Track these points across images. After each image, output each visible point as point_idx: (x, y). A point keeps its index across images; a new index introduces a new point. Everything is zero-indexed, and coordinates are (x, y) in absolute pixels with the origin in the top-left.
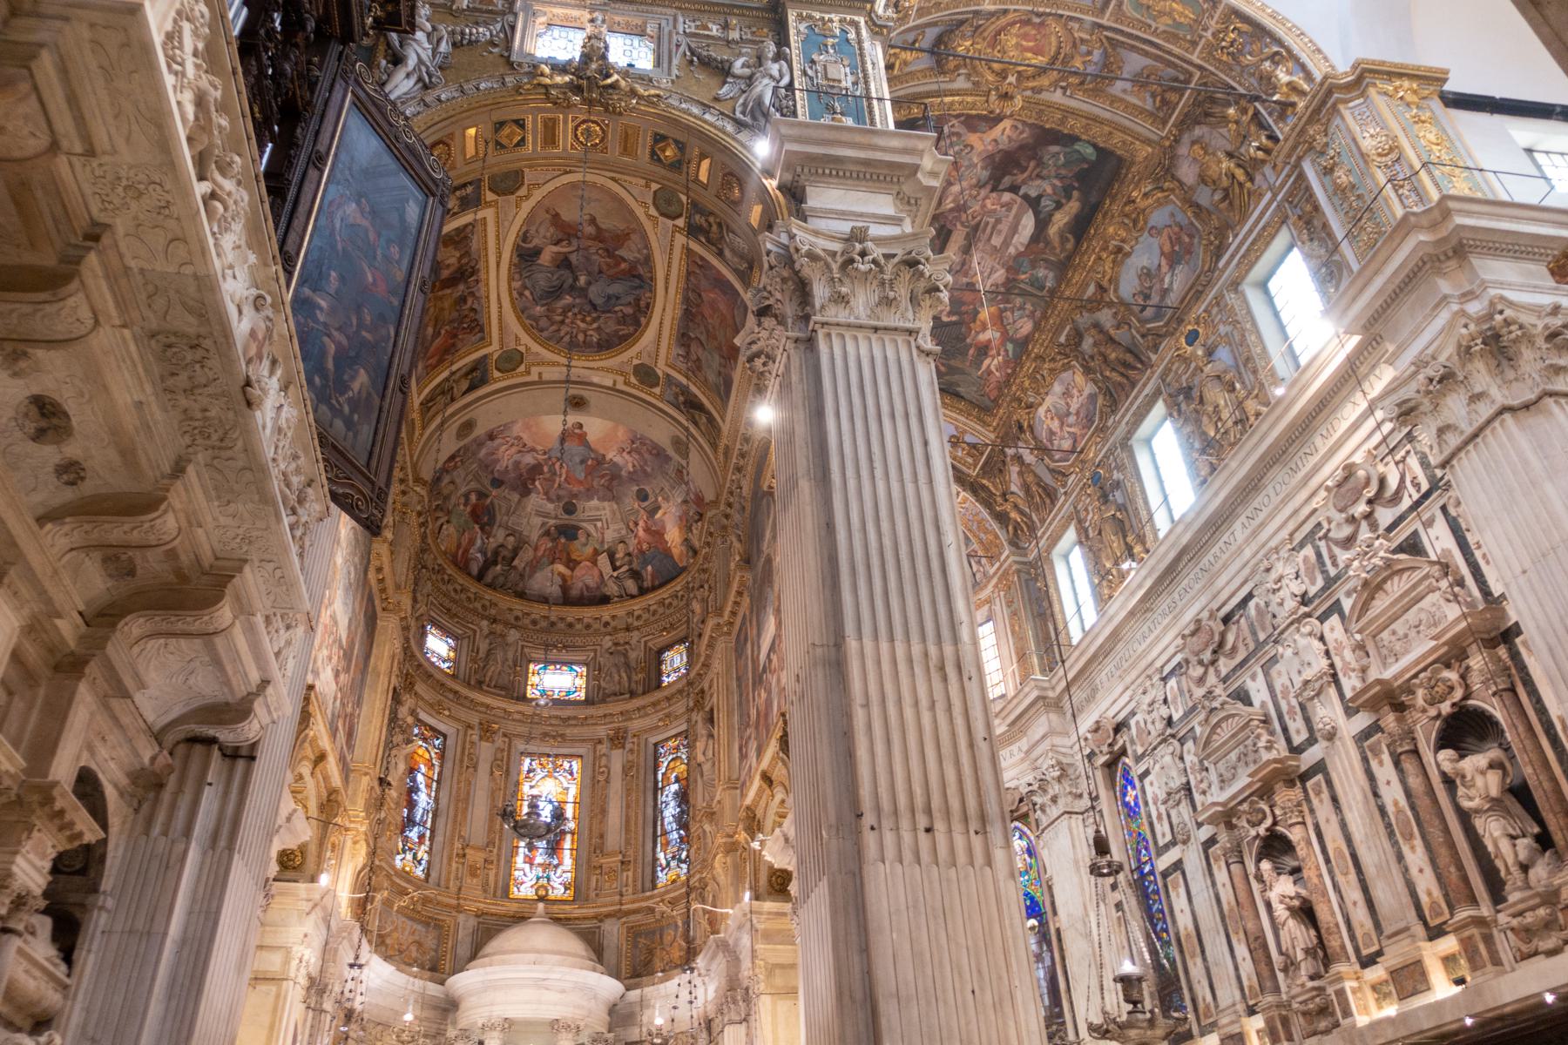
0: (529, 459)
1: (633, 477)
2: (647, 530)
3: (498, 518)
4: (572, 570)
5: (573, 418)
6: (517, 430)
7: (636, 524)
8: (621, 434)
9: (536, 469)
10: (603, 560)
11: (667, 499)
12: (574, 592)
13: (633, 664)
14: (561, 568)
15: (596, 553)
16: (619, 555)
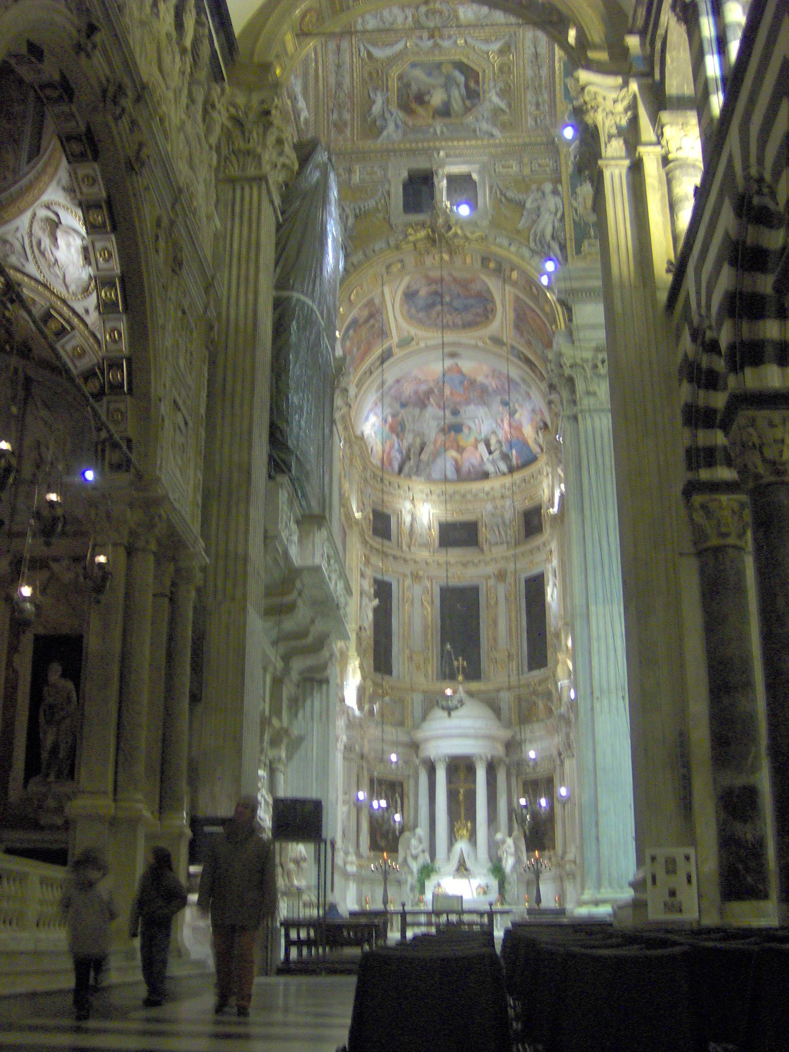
0: (423, 388)
1: (497, 392)
2: (510, 425)
3: (407, 427)
4: (461, 454)
5: (449, 363)
6: (415, 372)
7: (502, 421)
8: (485, 368)
9: (430, 392)
10: (482, 448)
11: (521, 406)
12: (465, 469)
13: (508, 522)
14: (453, 453)
15: (477, 441)
16: (493, 441)
